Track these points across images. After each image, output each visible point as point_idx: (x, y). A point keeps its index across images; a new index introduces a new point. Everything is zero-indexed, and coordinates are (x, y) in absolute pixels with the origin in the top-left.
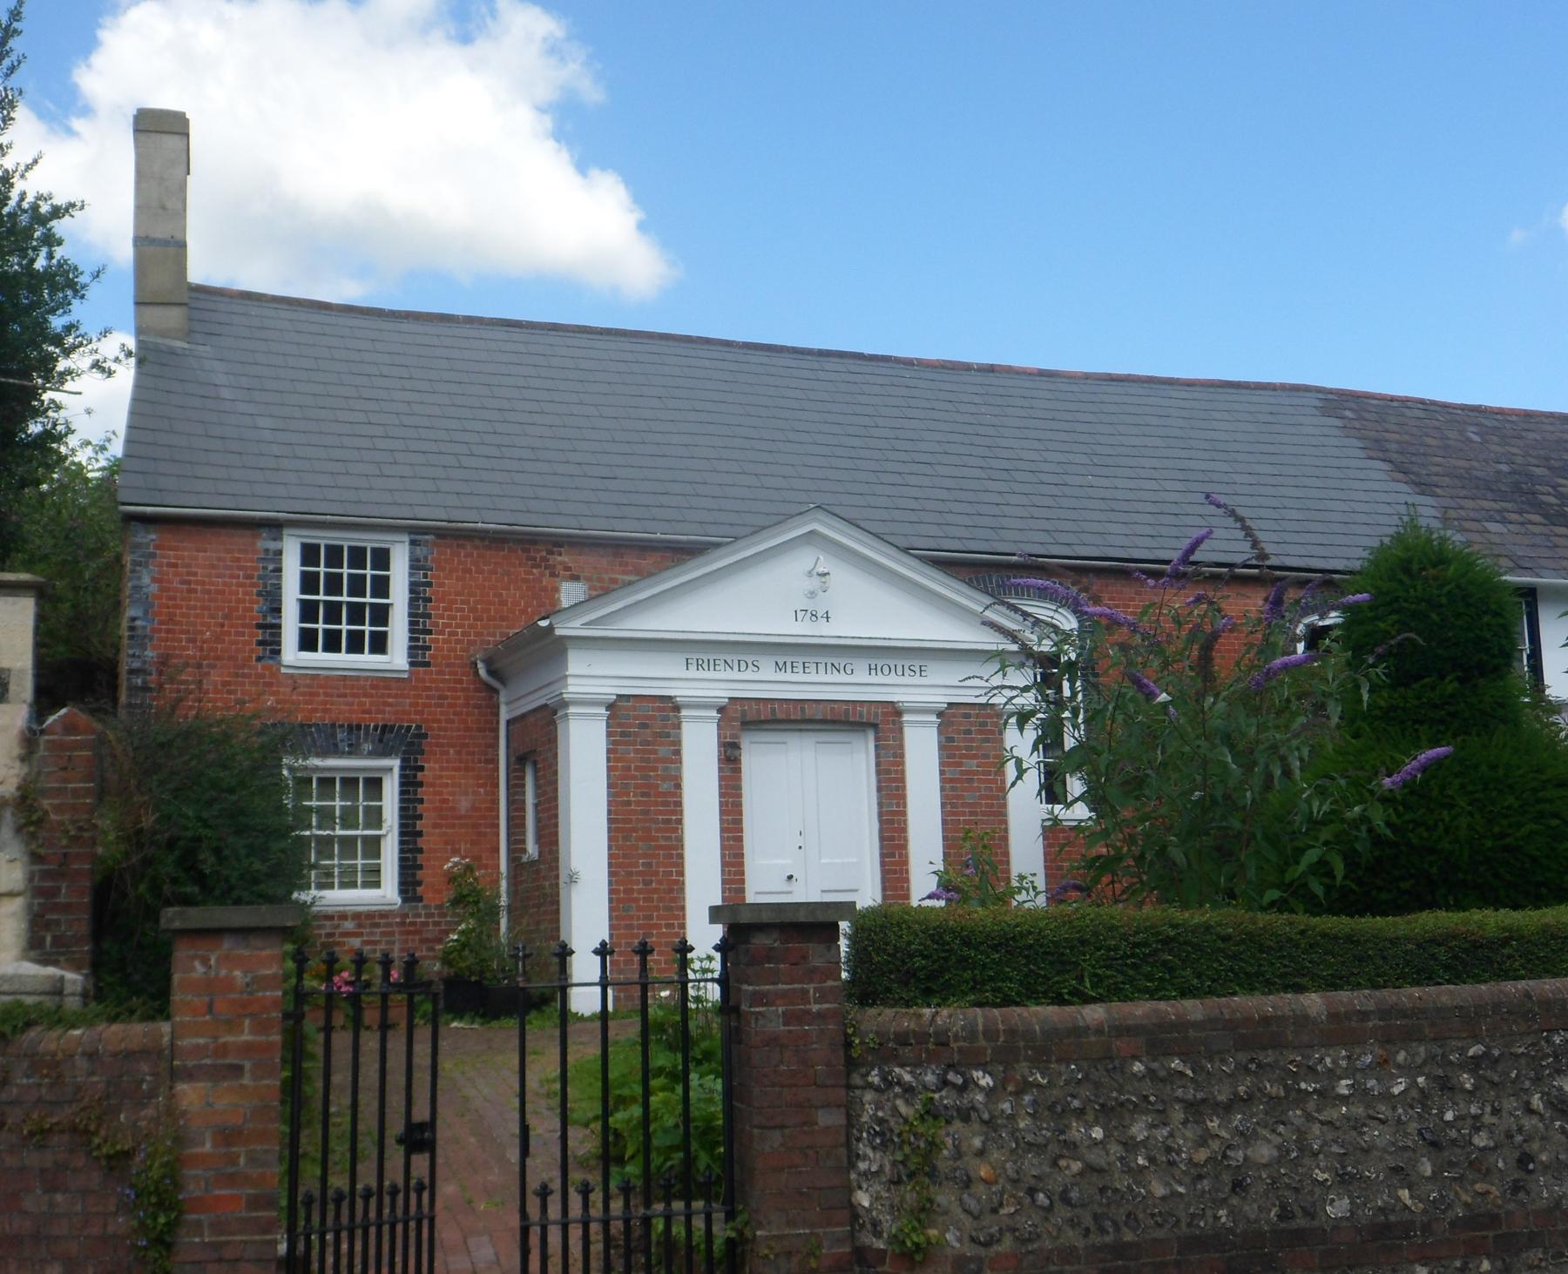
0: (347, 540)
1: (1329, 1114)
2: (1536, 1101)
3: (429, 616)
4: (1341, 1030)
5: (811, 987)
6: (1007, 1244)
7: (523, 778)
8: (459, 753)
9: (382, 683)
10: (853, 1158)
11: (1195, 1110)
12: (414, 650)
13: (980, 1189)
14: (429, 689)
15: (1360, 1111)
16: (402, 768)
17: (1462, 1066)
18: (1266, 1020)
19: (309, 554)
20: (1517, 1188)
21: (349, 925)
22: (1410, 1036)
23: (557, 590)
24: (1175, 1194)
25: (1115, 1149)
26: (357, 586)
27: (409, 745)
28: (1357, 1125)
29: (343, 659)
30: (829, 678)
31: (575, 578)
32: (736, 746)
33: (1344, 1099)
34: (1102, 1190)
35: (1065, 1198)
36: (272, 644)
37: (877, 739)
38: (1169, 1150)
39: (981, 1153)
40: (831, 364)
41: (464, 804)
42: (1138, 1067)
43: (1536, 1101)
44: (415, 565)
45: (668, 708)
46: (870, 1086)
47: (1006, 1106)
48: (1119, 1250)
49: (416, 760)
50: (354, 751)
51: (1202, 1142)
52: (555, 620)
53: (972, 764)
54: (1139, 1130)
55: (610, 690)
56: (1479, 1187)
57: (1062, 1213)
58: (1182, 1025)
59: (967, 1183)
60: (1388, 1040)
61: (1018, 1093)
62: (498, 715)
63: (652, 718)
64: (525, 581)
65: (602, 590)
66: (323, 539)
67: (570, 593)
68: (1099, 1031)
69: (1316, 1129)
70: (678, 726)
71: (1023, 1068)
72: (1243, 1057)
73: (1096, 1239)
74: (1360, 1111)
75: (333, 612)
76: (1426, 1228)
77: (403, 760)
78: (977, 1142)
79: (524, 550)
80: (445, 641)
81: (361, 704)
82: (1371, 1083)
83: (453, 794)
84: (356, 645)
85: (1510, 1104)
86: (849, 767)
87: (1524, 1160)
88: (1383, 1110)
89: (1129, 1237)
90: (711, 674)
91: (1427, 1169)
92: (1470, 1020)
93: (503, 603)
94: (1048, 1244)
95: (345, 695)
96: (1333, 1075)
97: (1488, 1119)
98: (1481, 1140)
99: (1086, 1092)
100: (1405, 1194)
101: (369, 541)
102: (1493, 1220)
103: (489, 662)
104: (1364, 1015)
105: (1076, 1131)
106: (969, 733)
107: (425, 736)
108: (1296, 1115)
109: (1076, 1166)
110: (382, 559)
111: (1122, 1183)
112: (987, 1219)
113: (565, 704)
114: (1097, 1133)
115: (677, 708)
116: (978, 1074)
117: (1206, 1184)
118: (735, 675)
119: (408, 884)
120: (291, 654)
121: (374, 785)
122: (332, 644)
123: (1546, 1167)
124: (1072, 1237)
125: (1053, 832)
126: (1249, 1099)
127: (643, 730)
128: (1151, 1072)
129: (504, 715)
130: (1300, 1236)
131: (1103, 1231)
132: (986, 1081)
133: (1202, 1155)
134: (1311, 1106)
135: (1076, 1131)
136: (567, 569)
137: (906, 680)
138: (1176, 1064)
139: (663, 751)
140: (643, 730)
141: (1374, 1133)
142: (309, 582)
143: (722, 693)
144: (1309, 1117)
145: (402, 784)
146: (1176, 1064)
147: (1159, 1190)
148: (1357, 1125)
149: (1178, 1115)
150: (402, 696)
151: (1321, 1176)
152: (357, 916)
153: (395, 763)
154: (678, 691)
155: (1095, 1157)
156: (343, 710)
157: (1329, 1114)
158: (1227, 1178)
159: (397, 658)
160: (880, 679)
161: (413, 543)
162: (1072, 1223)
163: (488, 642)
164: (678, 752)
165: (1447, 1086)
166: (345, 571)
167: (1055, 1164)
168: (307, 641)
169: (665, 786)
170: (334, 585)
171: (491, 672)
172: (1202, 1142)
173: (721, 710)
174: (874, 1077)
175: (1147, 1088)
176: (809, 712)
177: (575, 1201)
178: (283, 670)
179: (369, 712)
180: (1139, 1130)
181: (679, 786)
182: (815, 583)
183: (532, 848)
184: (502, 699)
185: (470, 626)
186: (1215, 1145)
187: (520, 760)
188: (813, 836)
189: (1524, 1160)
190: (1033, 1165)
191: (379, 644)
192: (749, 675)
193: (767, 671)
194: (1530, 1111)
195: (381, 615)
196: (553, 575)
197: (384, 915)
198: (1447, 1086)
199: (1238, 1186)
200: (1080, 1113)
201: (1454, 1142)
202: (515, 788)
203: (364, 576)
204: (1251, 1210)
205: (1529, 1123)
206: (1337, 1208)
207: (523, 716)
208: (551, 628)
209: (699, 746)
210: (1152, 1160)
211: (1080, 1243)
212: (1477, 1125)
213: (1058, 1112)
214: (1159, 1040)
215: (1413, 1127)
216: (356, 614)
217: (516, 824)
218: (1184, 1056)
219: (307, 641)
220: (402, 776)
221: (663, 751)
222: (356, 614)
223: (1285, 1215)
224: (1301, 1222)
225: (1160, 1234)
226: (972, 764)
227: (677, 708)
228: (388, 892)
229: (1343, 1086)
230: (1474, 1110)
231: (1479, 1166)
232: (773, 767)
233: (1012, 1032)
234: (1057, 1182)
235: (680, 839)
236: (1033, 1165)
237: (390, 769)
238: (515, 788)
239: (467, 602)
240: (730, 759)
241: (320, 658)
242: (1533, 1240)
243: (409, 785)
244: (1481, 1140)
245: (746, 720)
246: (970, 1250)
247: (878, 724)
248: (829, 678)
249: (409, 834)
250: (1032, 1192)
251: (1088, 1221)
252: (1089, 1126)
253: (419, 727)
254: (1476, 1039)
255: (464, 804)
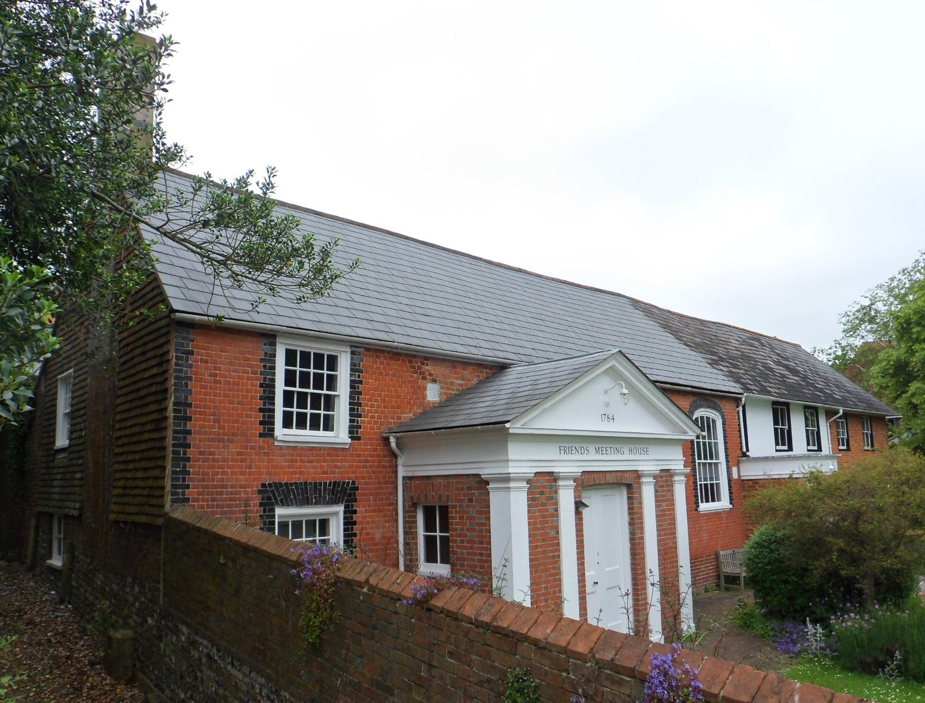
0: (313, 348)
3: (360, 404)
7: (415, 517)
8: (375, 500)
9: (334, 451)
14: (359, 456)
16: (345, 512)
19: (290, 357)
23: (425, 388)
31: (434, 381)
37: (628, 493)
41: (378, 536)
44: (354, 369)
45: (553, 477)
49: (352, 506)
55: (529, 470)
62: (396, 472)
63: (545, 487)
64: (410, 382)
66: (299, 346)
70: (556, 492)
77: (346, 507)
79: (410, 362)
80: (369, 422)
81: (322, 467)
83: (372, 528)
84: (315, 426)
93: (399, 397)
95: (312, 461)
101: (326, 350)
107: (357, 489)
110: (333, 362)
120: (280, 431)
122: (301, 424)
129: (401, 473)
136: (431, 375)
142: (290, 379)
145: (345, 524)
150: (345, 461)
153: (340, 509)
156: (312, 473)
159: (340, 434)
161: (352, 353)
163: (391, 423)
164: (556, 510)
178: (276, 443)
179: (326, 473)
181: (558, 533)
184: (400, 462)
185: (382, 412)
195: (330, 402)
196: (424, 378)
203: (309, 373)
207: (428, 477)
219: (287, 424)
220: (345, 518)
237: (336, 514)
239: (379, 395)
243: (349, 523)
253: (354, 483)
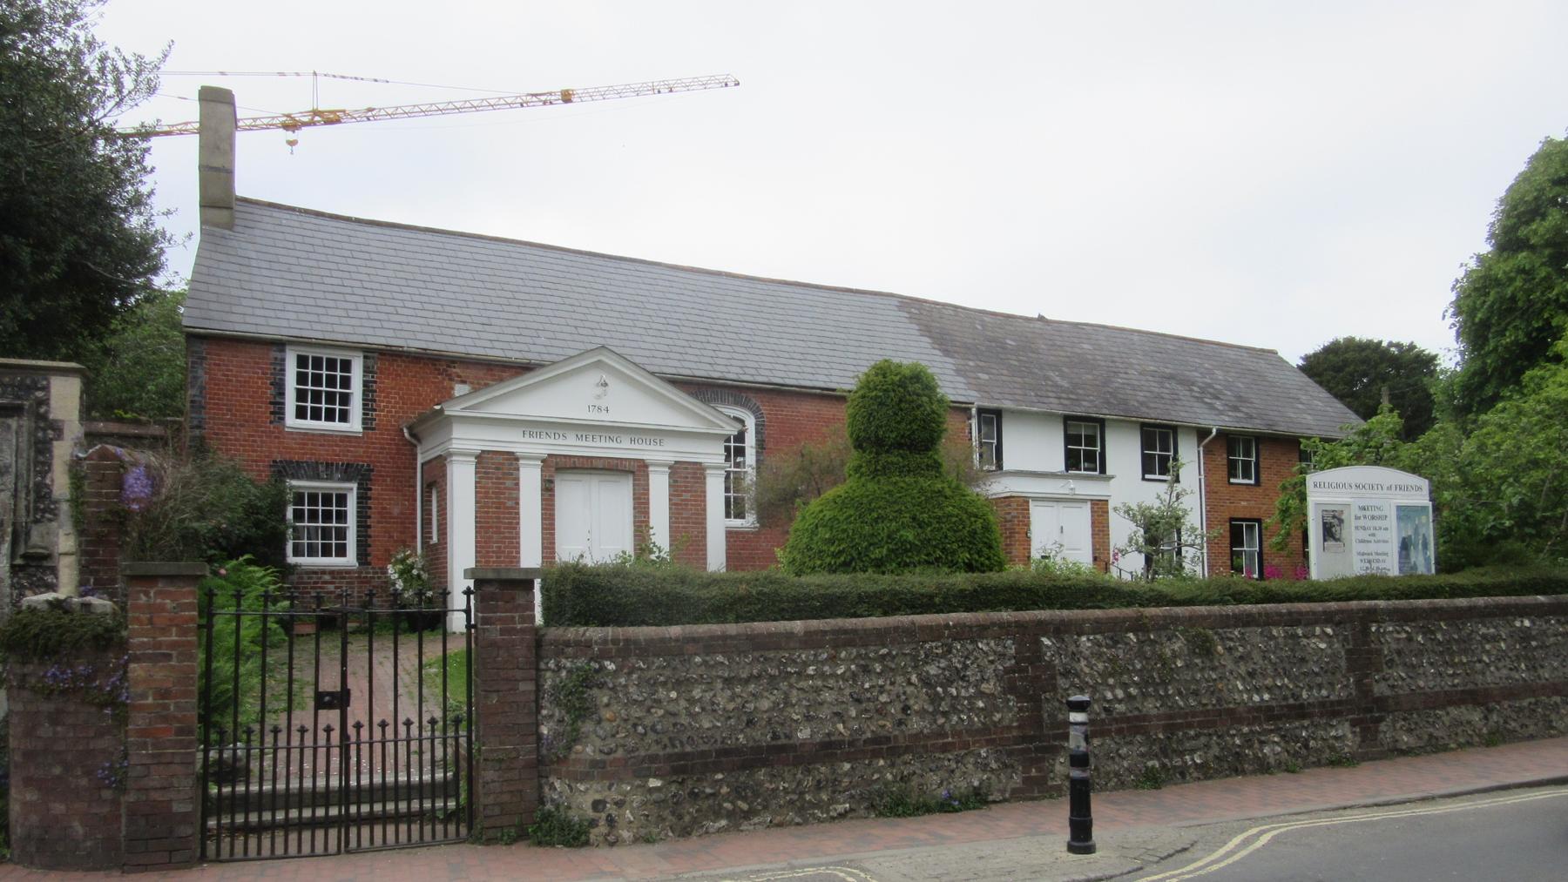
1: (802, 684)
2: (914, 678)
4: (811, 641)
5: (517, 615)
6: (620, 753)
9: (347, 439)
10: (539, 708)
11: (728, 682)
12: (365, 421)
13: (606, 725)
15: (819, 683)
17: (874, 660)
18: (771, 635)
20: (900, 723)
21: (327, 577)
22: (849, 643)
24: (715, 727)
25: (683, 703)
26: (331, 381)
27: (361, 474)
28: (817, 690)
29: (322, 425)
30: (603, 444)
31: (464, 382)
32: (552, 482)
33: (812, 677)
34: (675, 725)
35: (653, 729)
36: (279, 413)
38: (713, 703)
39: (607, 705)
40: (624, 265)
41: (396, 511)
42: (698, 659)
43: (914, 678)
44: (367, 370)
45: (512, 459)
46: (549, 669)
47: (623, 681)
48: (683, 756)
50: (330, 478)
51: (732, 699)
52: (445, 406)
53: (687, 496)
54: (697, 693)
55: (478, 447)
56: (881, 722)
57: (652, 736)
58: (725, 637)
59: (599, 722)
60: (837, 646)
61: (630, 674)
65: (477, 389)
67: (460, 389)
68: (677, 640)
69: (795, 692)
71: (633, 660)
72: (756, 654)
73: (669, 750)
74: (819, 683)
75: (316, 397)
76: (851, 744)
78: (605, 700)
82: (826, 668)
84: (330, 416)
85: (900, 679)
86: (616, 498)
87: (905, 709)
88: (831, 683)
89: (688, 749)
90: (538, 440)
91: (853, 713)
92: (881, 636)
94: (643, 753)
96: (806, 664)
97: (888, 687)
98: (884, 698)
99: (668, 672)
100: (840, 726)
102: (888, 739)
103: (410, 429)
104: (824, 633)
105: (662, 693)
106: (687, 479)
108: (784, 685)
109: (661, 712)
110: (346, 366)
111: (684, 720)
112: (609, 741)
113: (451, 454)
114: (673, 695)
115: (517, 459)
116: (607, 663)
117: (732, 721)
118: (552, 441)
119: (363, 555)
121: (342, 500)
122: (316, 415)
123: (917, 712)
124: (655, 749)
125: (731, 535)
126: (759, 677)
127: (497, 473)
128: (705, 663)
130: (783, 748)
131: (674, 746)
132: (611, 666)
133: (731, 706)
134: (793, 680)
135: (662, 693)
137: (652, 447)
138: (720, 658)
139: (509, 483)
140: (497, 473)
141: (827, 696)
143: (544, 451)
144: (791, 686)
146: (720, 658)
147: (707, 725)
148: (817, 690)
149: (720, 685)
151: (795, 717)
152: (332, 573)
153: (355, 486)
154: (517, 449)
155: (671, 708)
157: (802, 684)
158: (745, 718)
159: (355, 425)
160: (636, 446)
161: (365, 357)
162: (657, 742)
165: (866, 670)
166: (324, 372)
167: (648, 711)
168: (301, 413)
169: (509, 504)
170: (317, 380)
171: (412, 435)
172: (732, 699)
173: (543, 461)
174: (552, 664)
175: (702, 670)
176: (595, 464)
177: (402, 730)
180: (697, 693)
182: (600, 390)
183: (435, 539)
184: (419, 450)
186: (739, 700)
187: (429, 486)
188: (594, 530)
189: (905, 709)
190: (636, 712)
191: (344, 417)
192: (561, 442)
193: (571, 439)
194: (910, 683)
195: (345, 399)
196: (451, 380)
197: (348, 572)
198: (866, 670)
199: (750, 723)
200: (664, 684)
201: (869, 700)
202: (426, 502)
204: (757, 734)
205: (909, 690)
206: (803, 734)
208: (442, 411)
209: (530, 481)
210: (703, 709)
211: (661, 753)
212: (882, 690)
213: (654, 684)
214: (709, 645)
215: (847, 692)
216: (331, 398)
217: (427, 523)
218: (723, 653)
219: (301, 413)
221: (509, 483)
222: (331, 398)
223: (775, 737)
224: (783, 741)
225: (706, 748)
226: (687, 496)
227: (517, 459)
228: (350, 559)
229: (811, 670)
230: (881, 682)
231: (881, 711)
232: (570, 493)
233: (627, 641)
234: (647, 722)
235: (518, 533)
236: (636, 712)
238: (426, 502)
240: (548, 489)
241: (309, 424)
242: (907, 750)
243: (362, 499)
244: (884, 698)
245: (557, 468)
246: (598, 757)
247: (637, 471)
248: (603, 444)
249: (363, 526)
250: (635, 726)
251: (666, 740)
252: (669, 691)
254: (884, 646)
255: (396, 511)
